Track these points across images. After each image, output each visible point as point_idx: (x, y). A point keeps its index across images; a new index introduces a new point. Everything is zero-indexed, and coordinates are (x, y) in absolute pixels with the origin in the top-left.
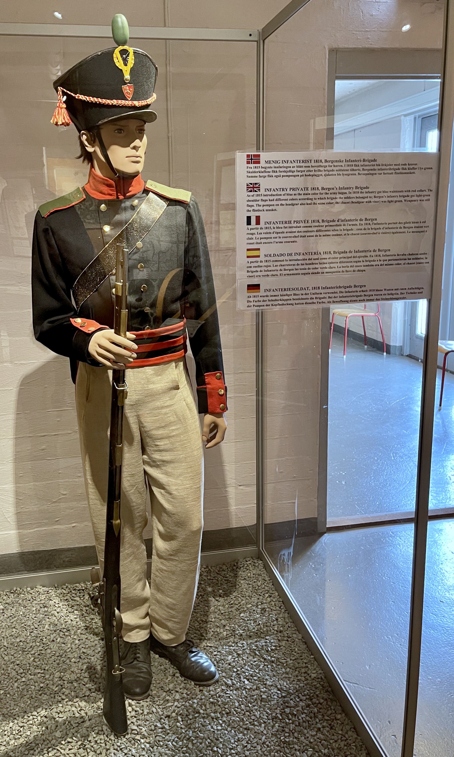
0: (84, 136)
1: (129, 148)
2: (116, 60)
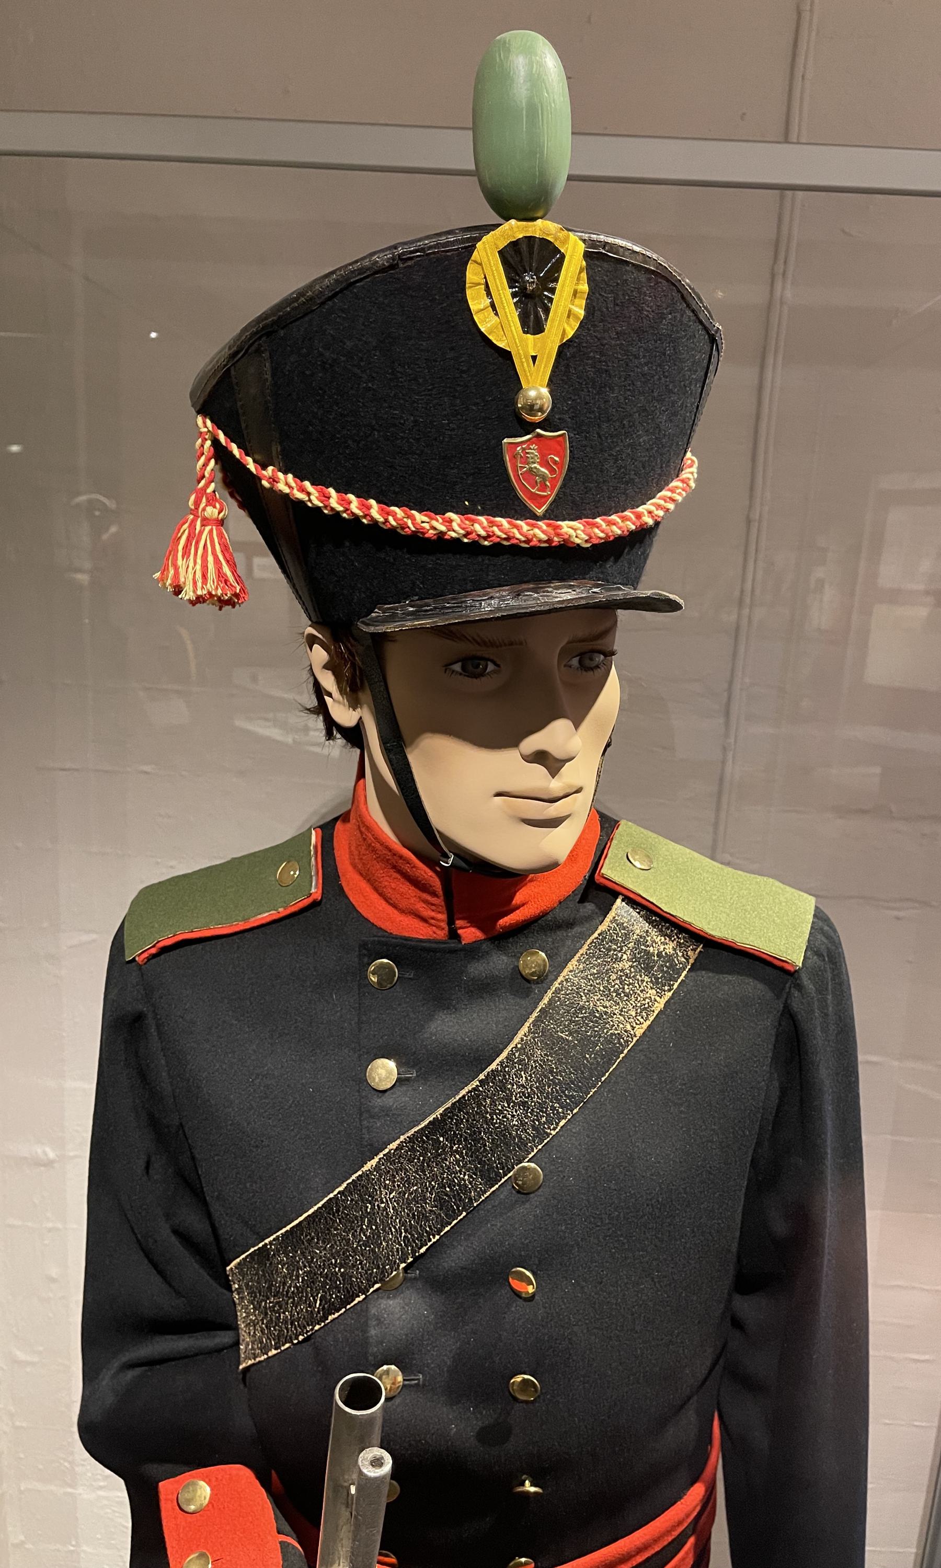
2: (476, 302)
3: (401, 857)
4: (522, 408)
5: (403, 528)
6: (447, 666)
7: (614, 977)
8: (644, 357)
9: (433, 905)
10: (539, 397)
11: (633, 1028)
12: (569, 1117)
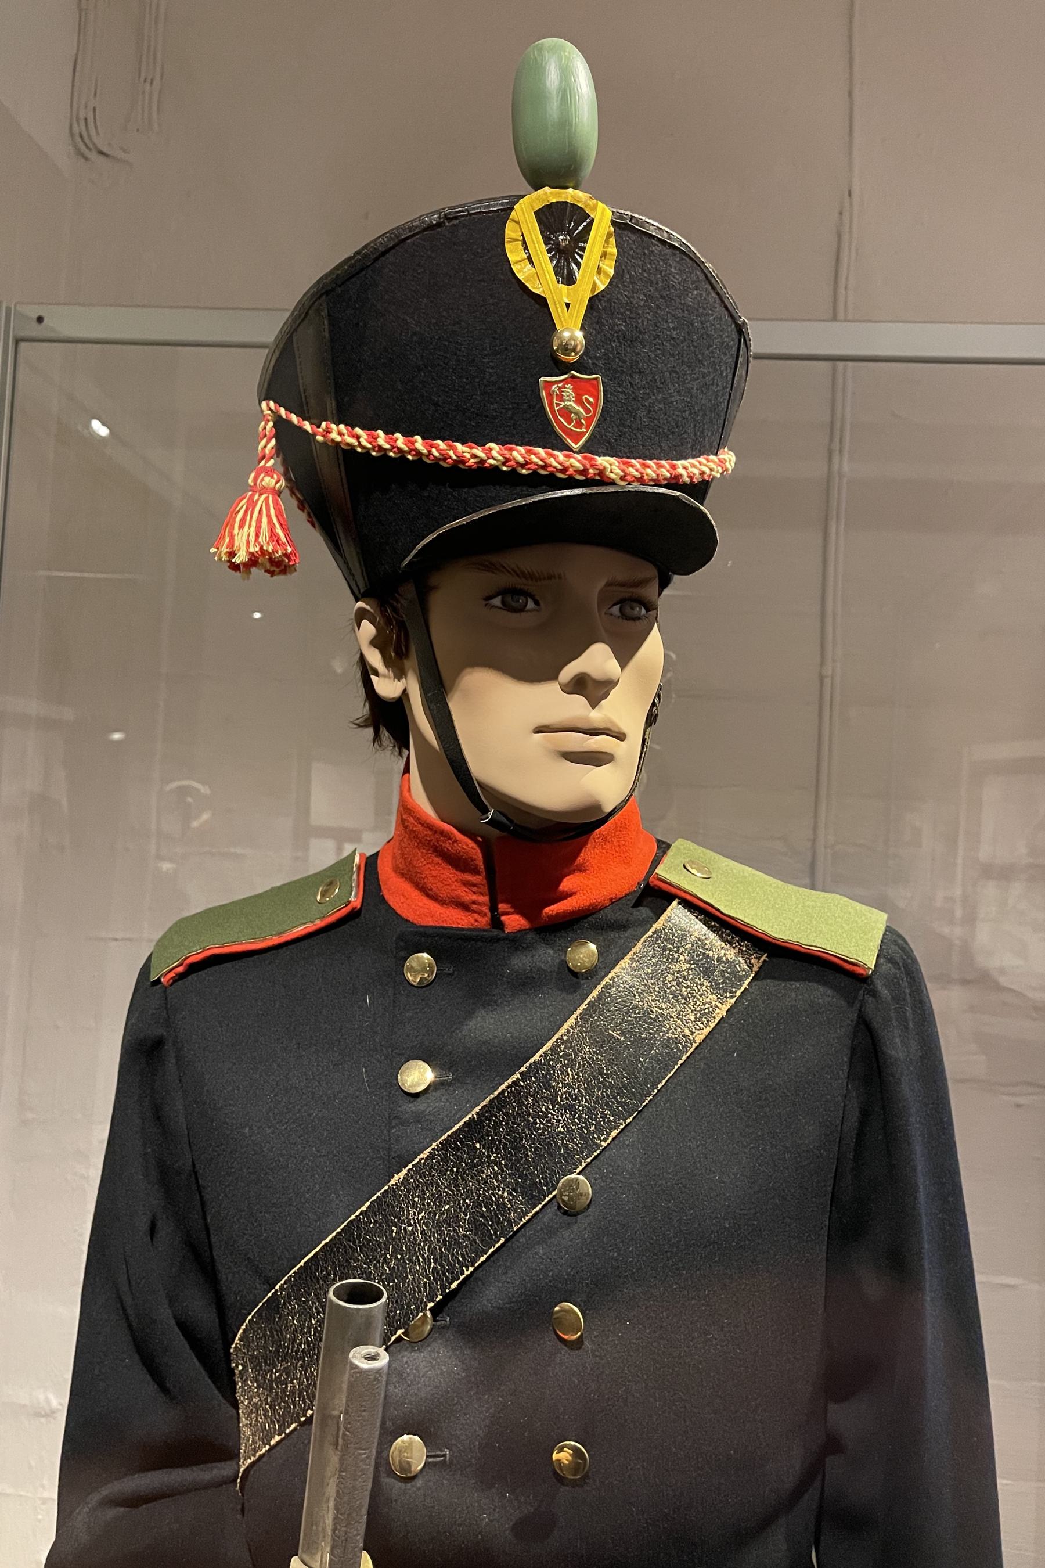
0: (365, 623)
1: (552, 689)
2: (514, 254)
3: (442, 833)
4: (557, 350)
5: (445, 459)
6: (489, 598)
7: (670, 978)
8: (672, 322)
9: (474, 885)
10: (572, 338)
11: (692, 1033)
12: (621, 1127)
